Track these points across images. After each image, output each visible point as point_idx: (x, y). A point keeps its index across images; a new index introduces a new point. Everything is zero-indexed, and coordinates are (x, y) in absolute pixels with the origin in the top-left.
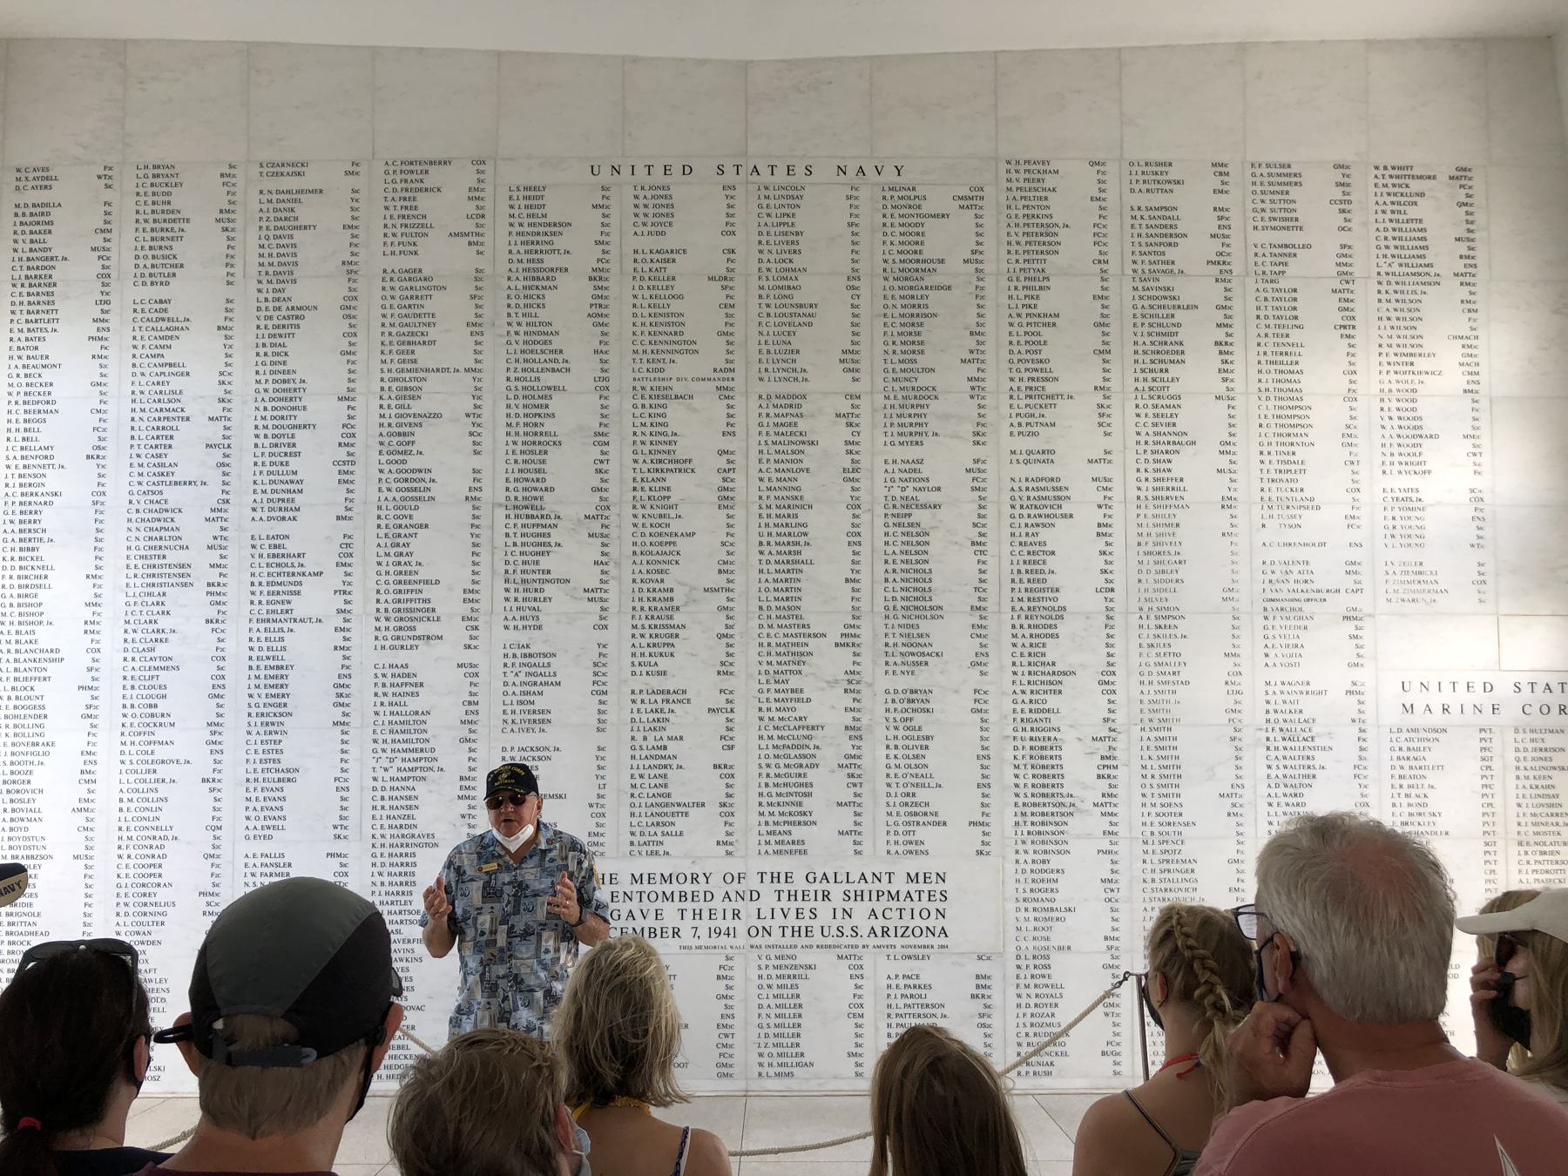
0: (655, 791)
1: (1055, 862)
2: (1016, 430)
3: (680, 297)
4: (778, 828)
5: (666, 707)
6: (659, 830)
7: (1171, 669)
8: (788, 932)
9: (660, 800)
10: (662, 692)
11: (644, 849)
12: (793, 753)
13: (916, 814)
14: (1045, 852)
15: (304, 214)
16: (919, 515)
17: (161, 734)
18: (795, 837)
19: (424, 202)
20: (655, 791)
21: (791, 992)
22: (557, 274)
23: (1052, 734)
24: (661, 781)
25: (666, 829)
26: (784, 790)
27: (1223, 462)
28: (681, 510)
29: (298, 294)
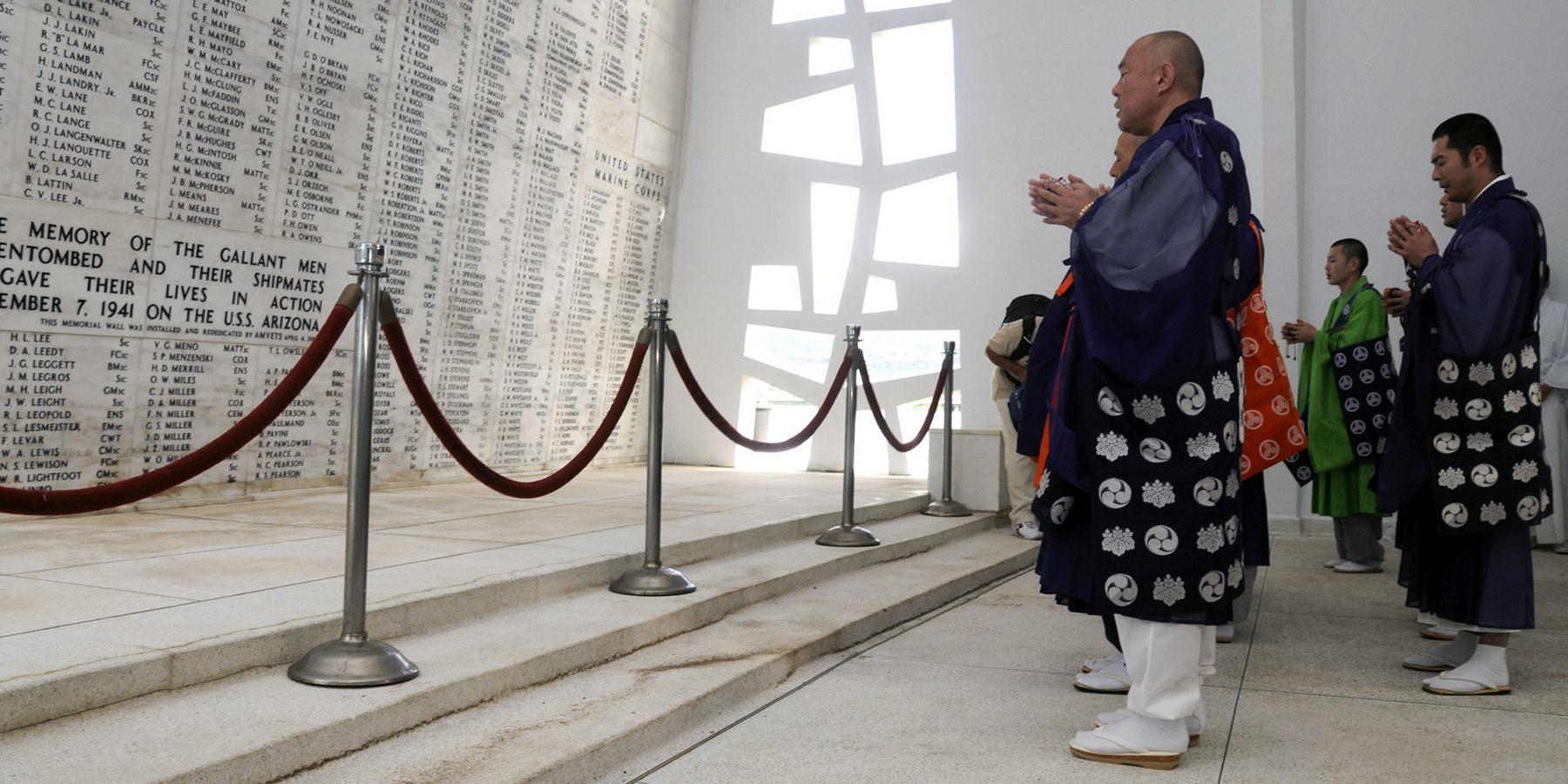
0: (70, 115)
4: (193, 190)
6: (69, 168)
8: (193, 314)
9: (73, 128)
11: (47, 191)
12: (222, 103)
13: (313, 197)
14: (400, 253)
18: (209, 203)
20: (70, 115)
21: (187, 386)
23: (420, 138)
24: (79, 103)
25: (78, 169)
26: (207, 146)
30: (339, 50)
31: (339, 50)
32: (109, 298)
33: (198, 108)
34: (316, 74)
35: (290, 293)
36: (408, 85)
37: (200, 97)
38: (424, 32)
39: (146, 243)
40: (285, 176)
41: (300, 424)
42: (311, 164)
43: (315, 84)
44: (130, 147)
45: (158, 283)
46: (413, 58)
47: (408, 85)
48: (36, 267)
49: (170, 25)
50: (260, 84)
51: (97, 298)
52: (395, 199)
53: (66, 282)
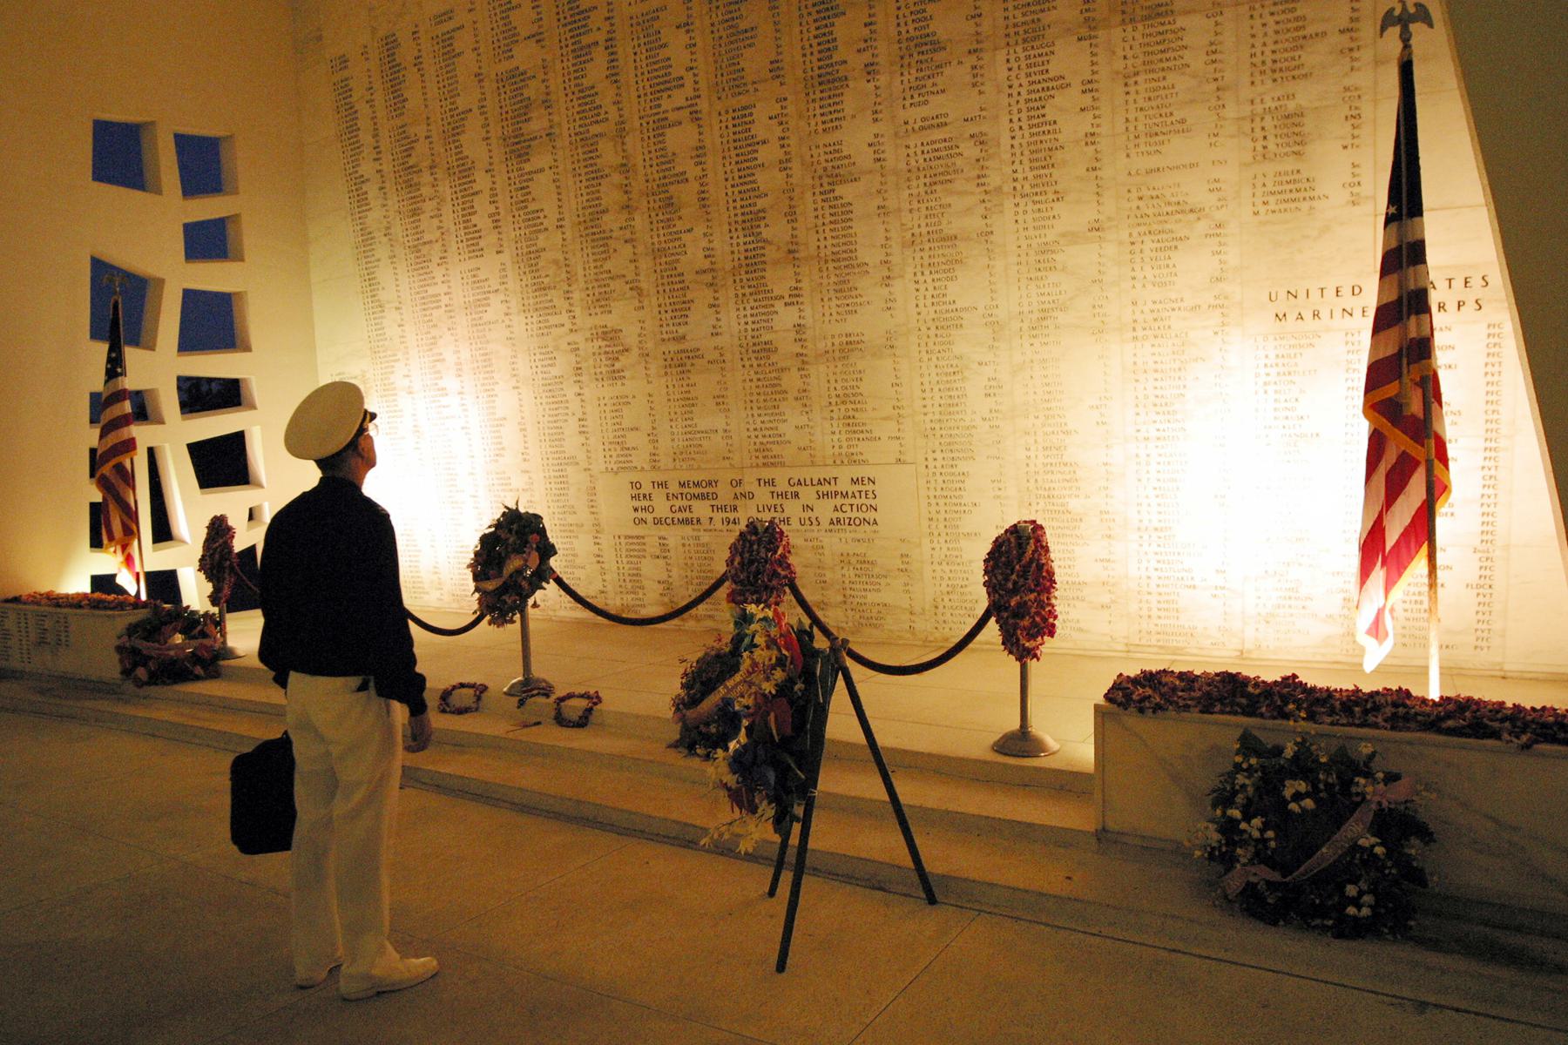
1: (963, 466)
2: (907, 103)
3: (665, 45)
5: (689, 362)
7: (1050, 299)
10: (683, 351)
15: (458, 46)
16: (840, 190)
17: (444, 401)
19: (515, 17)
22: (593, 49)
23: (954, 362)
27: (1087, 100)
28: (683, 212)
29: (462, 103)
30: (852, 325)
31: (852, 325)
32: (725, 515)
33: (755, 398)
34: (837, 347)
35: (847, 501)
36: (930, 324)
37: (755, 391)
38: (936, 276)
39: (740, 482)
40: (827, 425)
41: (879, 590)
42: (847, 410)
43: (837, 354)
44: (721, 433)
45: (752, 504)
46: (929, 301)
47: (930, 324)
48: (685, 503)
49: (728, 356)
50: (794, 371)
51: (719, 516)
52: (937, 417)
53: (701, 509)
